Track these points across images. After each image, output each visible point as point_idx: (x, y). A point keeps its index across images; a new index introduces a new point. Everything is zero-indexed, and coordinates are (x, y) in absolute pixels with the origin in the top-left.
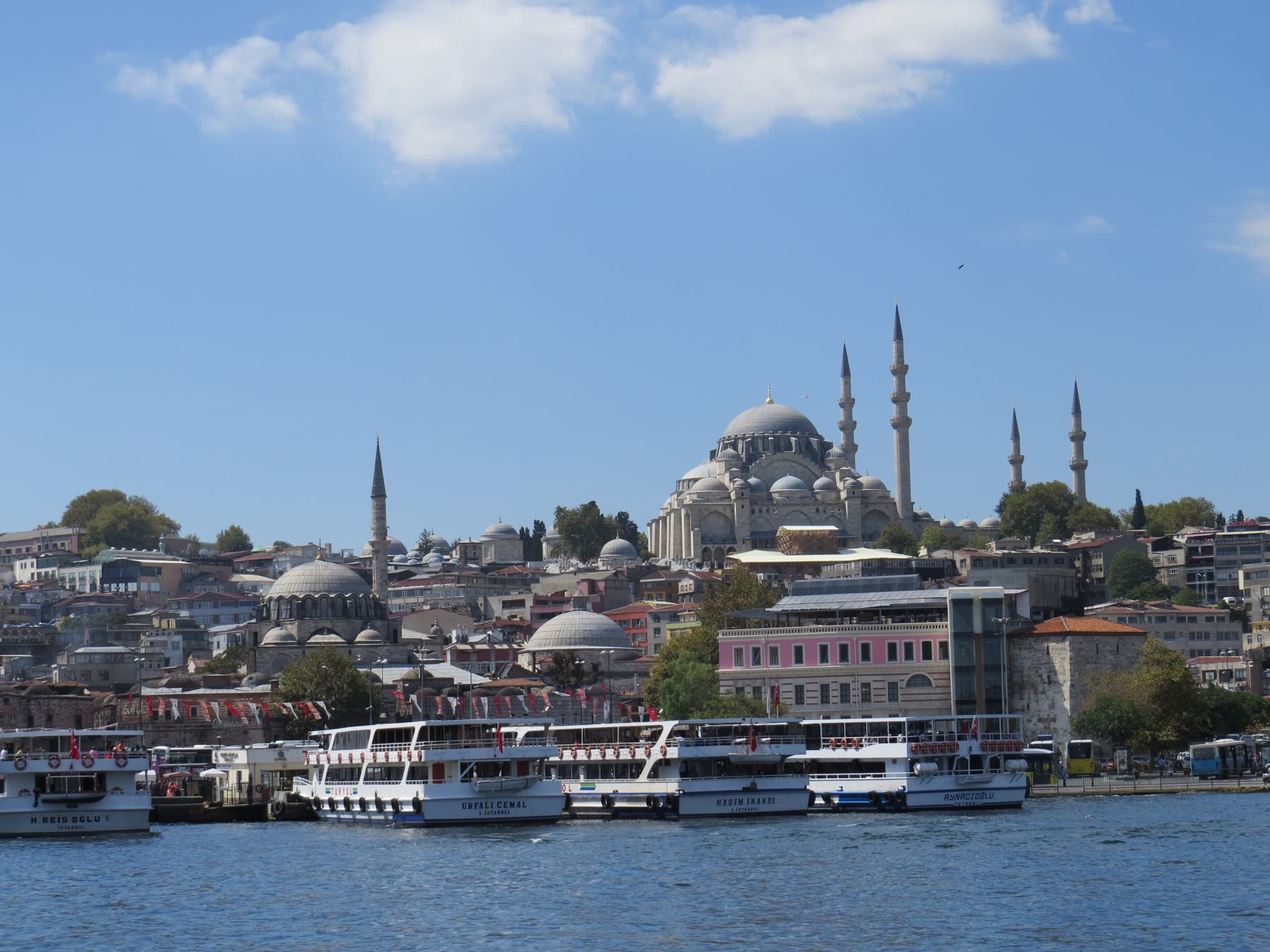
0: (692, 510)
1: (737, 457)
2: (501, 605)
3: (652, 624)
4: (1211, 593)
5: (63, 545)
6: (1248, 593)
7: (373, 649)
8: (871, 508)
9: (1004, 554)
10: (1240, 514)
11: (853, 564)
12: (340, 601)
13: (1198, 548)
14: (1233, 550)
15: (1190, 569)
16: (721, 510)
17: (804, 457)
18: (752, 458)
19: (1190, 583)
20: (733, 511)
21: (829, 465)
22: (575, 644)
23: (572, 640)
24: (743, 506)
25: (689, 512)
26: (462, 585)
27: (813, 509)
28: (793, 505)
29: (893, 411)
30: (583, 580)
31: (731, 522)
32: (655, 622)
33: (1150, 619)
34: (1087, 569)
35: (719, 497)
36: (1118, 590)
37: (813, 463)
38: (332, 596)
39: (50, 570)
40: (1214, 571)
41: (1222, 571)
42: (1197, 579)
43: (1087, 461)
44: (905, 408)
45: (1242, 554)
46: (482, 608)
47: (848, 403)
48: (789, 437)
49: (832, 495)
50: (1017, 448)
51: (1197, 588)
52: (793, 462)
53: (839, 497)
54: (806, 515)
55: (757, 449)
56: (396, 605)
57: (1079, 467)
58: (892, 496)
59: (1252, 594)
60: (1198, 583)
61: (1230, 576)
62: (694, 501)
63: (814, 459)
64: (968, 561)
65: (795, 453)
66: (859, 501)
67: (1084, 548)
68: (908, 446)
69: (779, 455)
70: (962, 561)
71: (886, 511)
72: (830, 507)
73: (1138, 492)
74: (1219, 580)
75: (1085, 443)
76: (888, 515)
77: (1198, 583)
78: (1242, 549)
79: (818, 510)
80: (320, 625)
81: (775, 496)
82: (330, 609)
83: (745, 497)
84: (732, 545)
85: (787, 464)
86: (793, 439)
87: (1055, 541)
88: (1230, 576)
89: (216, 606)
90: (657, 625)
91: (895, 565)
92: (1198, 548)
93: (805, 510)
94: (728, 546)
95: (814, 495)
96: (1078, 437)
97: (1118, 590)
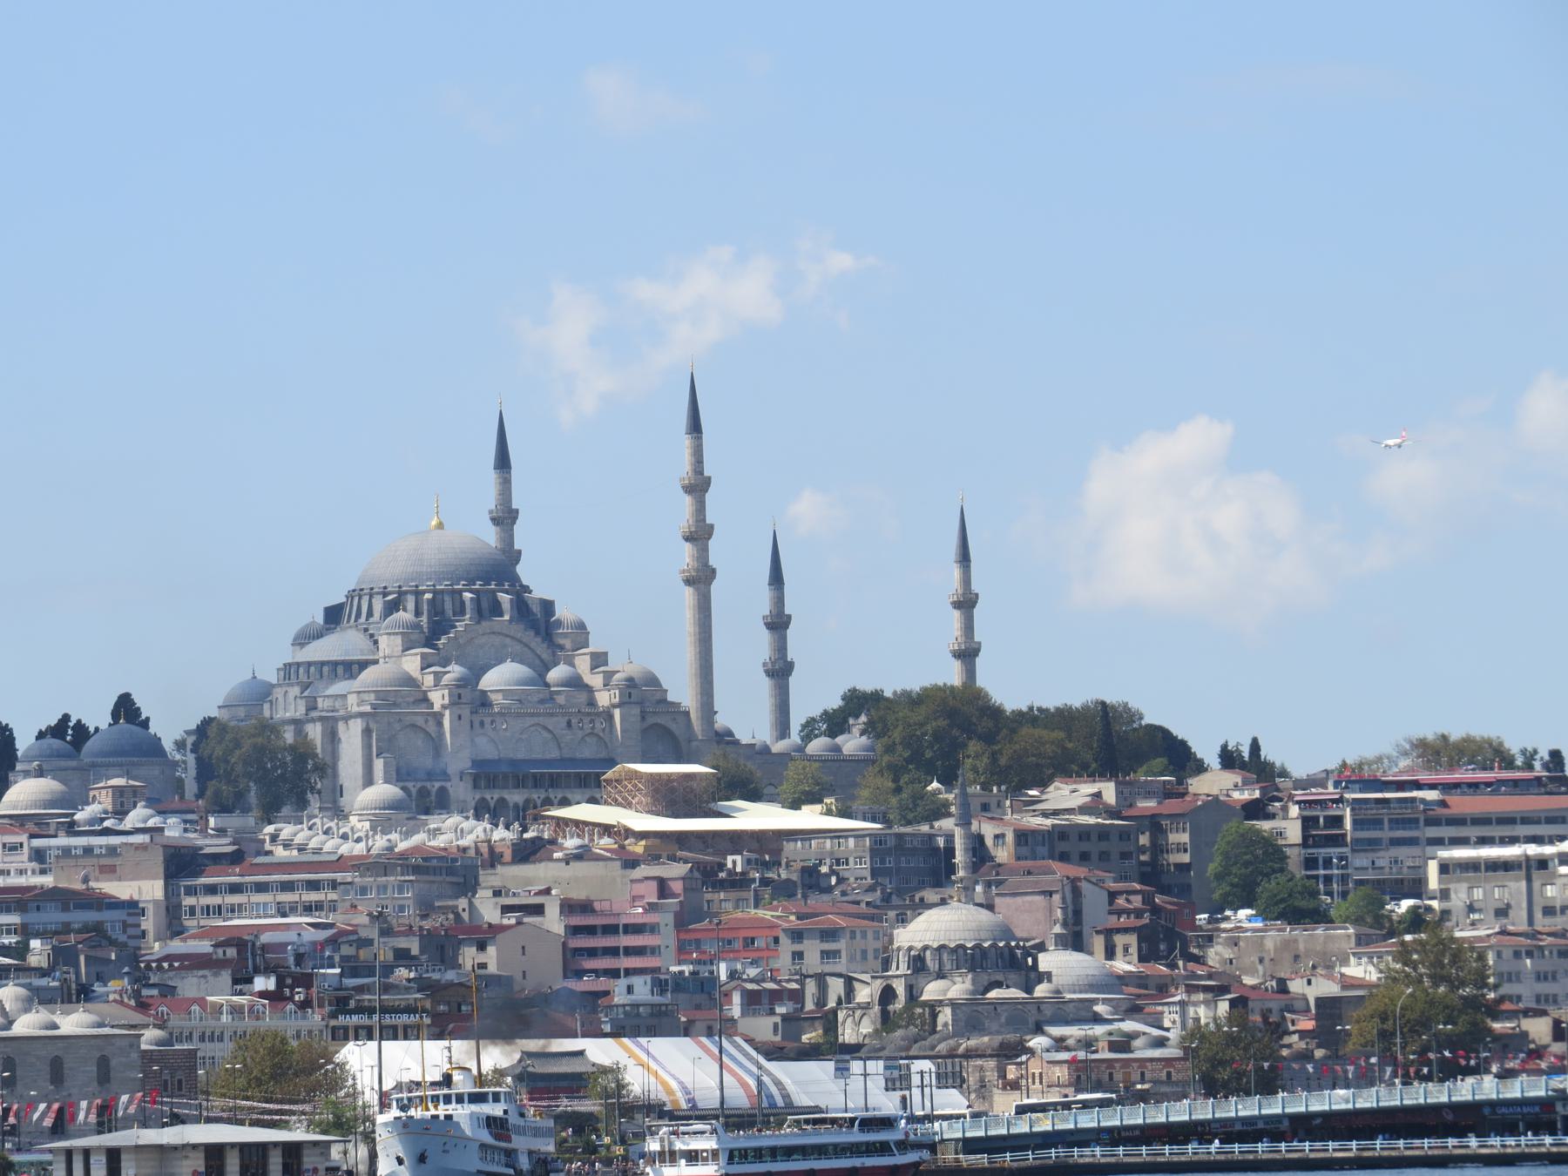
0: (377, 722)
1: (417, 626)
2: (499, 911)
3: (787, 946)
4: (1345, 888)
6: (1444, 895)
7: (1061, 1006)
8: (651, 720)
9: (1053, 826)
10: (1344, 762)
11: (851, 841)
12: (1007, 949)
13: (1317, 818)
14: (1376, 823)
15: (1310, 851)
16: (420, 721)
17: (525, 630)
18: (439, 627)
19: (1309, 873)
20: (440, 724)
21: (561, 641)
22: (1081, 992)
23: (1077, 988)
24: (460, 717)
25: (373, 726)
26: (407, 878)
27: (563, 721)
28: (532, 715)
30: (647, 878)
31: (436, 743)
32: (793, 943)
33: (1551, 953)
34: (1158, 848)
35: (412, 700)
36: (1232, 885)
37: (539, 640)
40: (1349, 855)
41: (1362, 854)
42: (1335, 867)
43: (980, 643)
45: (1391, 829)
46: (465, 916)
47: (505, 518)
48: (494, 592)
49: (582, 697)
50: (779, 601)
51: (1321, 880)
52: (507, 636)
53: (592, 703)
54: (550, 731)
55: (443, 612)
56: (258, 904)
57: (967, 654)
58: (670, 698)
59: (1453, 896)
60: (1322, 872)
61: (1373, 862)
62: (374, 707)
63: (537, 633)
64: (1010, 838)
65: (510, 621)
66: (636, 711)
67: (1153, 816)
68: (709, 616)
69: (485, 624)
70: (997, 837)
71: (673, 727)
72: (586, 720)
74: (1356, 869)
75: (976, 611)
76: (677, 732)
77: (1322, 872)
78: (1390, 821)
79: (569, 724)
81: (497, 699)
82: (999, 961)
83: (463, 700)
84: (443, 784)
85: (497, 640)
86: (467, 595)
87: (1031, 792)
88: (1373, 862)
89: (65, 909)
90: (798, 947)
91: (915, 843)
92: (1317, 818)
93: (550, 723)
94: (437, 785)
95: (551, 698)
96: (966, 603)
97: (1232, 885)
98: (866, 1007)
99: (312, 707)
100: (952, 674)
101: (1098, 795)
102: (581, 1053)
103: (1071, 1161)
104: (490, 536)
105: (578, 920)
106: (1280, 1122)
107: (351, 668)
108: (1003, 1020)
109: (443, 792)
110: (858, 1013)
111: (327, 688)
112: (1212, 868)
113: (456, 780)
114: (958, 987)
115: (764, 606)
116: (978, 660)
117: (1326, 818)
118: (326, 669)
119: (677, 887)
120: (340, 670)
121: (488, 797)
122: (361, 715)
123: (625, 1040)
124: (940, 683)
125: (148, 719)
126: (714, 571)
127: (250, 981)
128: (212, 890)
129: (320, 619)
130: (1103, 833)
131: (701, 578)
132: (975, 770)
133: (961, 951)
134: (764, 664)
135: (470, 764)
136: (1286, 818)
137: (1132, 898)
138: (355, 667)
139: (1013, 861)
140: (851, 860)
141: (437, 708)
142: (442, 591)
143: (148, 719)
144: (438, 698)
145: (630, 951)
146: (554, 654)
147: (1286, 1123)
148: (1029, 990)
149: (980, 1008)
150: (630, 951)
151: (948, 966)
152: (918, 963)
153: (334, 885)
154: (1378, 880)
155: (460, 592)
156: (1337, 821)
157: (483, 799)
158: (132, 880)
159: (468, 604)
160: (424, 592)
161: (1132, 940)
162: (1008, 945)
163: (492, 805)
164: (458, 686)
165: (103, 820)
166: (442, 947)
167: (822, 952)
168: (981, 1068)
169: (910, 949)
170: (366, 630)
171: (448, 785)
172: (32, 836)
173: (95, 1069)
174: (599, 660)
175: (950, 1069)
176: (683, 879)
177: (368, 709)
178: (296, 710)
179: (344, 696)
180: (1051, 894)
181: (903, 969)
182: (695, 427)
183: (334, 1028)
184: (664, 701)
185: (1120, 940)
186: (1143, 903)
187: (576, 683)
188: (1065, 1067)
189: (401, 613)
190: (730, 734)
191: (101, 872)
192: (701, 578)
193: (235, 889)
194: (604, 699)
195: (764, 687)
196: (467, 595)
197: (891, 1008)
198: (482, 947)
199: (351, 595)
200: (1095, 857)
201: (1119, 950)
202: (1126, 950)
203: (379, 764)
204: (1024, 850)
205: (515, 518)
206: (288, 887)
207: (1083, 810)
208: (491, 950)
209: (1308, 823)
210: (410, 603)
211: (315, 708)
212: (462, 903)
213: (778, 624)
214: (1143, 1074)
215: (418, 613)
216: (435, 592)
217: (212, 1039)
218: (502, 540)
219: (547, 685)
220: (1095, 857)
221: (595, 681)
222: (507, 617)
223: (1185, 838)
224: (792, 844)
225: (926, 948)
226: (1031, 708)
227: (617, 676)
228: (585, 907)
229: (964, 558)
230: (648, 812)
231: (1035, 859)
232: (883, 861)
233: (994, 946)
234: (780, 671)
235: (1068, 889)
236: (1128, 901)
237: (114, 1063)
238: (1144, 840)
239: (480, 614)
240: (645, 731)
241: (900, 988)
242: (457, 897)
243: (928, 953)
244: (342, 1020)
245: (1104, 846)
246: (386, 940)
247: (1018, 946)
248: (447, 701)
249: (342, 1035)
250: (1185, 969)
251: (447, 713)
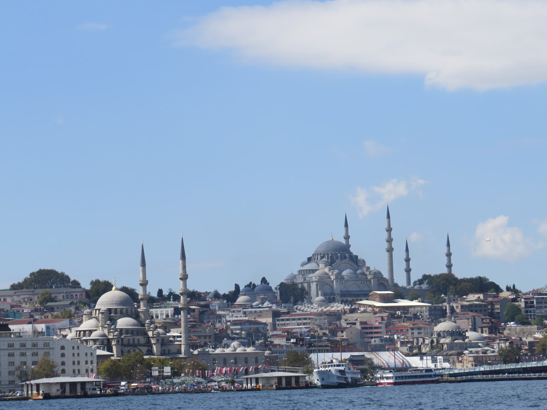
3: (410, 331)
5: (76, 295)
8: (380, 282)
9: (469, 304)
11: (424, 308)
14: (541, 303)
16: (329, 282)
20: (333, 283)
25: (318, 283)
27: (360, 282)
29: (386, 245)
31: (332, 287)
34: (493, 309)
36: (509, 317)
37: (355, 264)
38: (454, 330)
44: (391, 244)
45: (545, 304)
46: (339, 325)
47: (347, 237)
48: (344, 254)
49: (364, 277)
53: (366, 278)
56: (293, 323)
57: (449, 266)
58: (384, 277)
60: (529, 314)
62: (318, 279)
63: (354, 263)
64: (460, 307)
66: (376, 280)
67: (491, 302)
69: (343, 261)
70: (457, 307)
71: (384, 283)
76: (385, 284)
77: (529, 314)
78: (544, 302)
79: (362, 283)
80: (456, 338)
81: (345, 277)
89: (250, 324)
90: (412, 331)
92: (528, 302)
94: (333, 296)
95: (358, 277)
97: (509, 317)
98: (427, 345)
99: (305, 280)
100: (445, 271)
101: (479, 297)
102: (364, 355)
103: (473, 378)
104: (343, 241)
105: (363, 326)
106: (520, 369)
107: (313, 271)
108: (458, 347)
109: (334, 298)
110: (426, 346)
111: (308, 275)
112: (505, 313)
113: (337, 295)
114: (448, 340)
115: (404, 256)
116: (452, 268)
117: (530, 302)
118: (308, 271)
119: (386, 318)
120: (311, 271)
121: (344, 299)
122: (316, 281)
123: (374, 352)
124: (444, 273)
125: (269, 283)
126: (393, 249)
127: (290, 340)
128: (283, 320)
129: (306, 260)
130: (480, 306)
131: (390, 250)
132: (452, 292)
133: (448, 332)
134: (405, 269)
135: (339, 292)
136: (521, 302)
137: (487, 320)
138: (314, 271)
139: (460, 312)
140: (424, 312)
141: (332, 279)
142: (333, 254)
143: (269, 283)
144: (333, 277)
145: (375, 333)
146: (358, 267)
147: (522, 370)
148: (464, 340)
149: (453, 345)
150: (375, 333)
151: (446, 335)
152: (439, 335)
153: (310, 319)
154: (542, 316)
155: (337, 254)
156: (533, 302)
157: (343, 300)
158: (265, 318)
159: (339, 257)
160: (329, 254)
161: (487, 329)
162: (459, 330)
163: (345, 301)
164: (337, 275)
165: (259, 305)
166: (334, 332)
167: (418, 333)
168: (453, 358)
169: (437, 331)
170: (317, 263)
171: (335, 296)
172: (243, 309)
173: (254, 360)
174: (368, 268)
175: (446, 358)
176: (387, 316)
177: (317, 280)
178: (302, 281)
179: (312, 277)
180: (469, 319)
181: (436, 336)
182: (388, 217)
183: (309, 350)
184: (382, 277)
185: (484, 329)
186: (490, 321)
187: (363, 274)
188: (472, 358)
189: (324, 259)
190: (397, 284)
191: (258, 316)
192: (390, 250)
193: (288, 320)
194: (369, 277)
195: (405, 274)
196: (339, 255)
197: (433, 345)
198: (342, 332)
199: (313, 255)
200: (479, 311)
201: (484, 331)
202: (486, 331)
203: (320, 292)
204: (463, 309)
205: (349, 238)
206: (299, 319)
207: (476, 300)
208: (344, 333)
209: (526, 303)
210: (326, 257)
211: (305, 280)
212: (338, 322)
213: (408, 260)
214: (490, 359)
215: (328, 259)
216: (332, 254)
217: (281, 353)
218: (346, 242)
219: (357, 274)
220: (479, 311)
221: (368, 273)
222: (348, 259)
223: (498, 306)
224: (411, 309)
225: (441, 331)
226: (464, 278)
227: (372, 272)
228: (365, 323)
229: (448, 245)
230: (379, 302)
231: (465, 311)
232: (431, 312)
233: (456, 331)
234: (408, 270)
235: (473, 318)
236: (486, 321)
237: (259, 359)
238: (489, 307)
239: (342, 259)
240: (378, 284)
241: (435, 340)
242: (337, 321)
243: (441, 332)
244: (311, 348)
245: (481, 308)
246: (321, 331)
247: (461, 331)
248: (334, 278)
249: (311, 352)
250: (499, 335)
251: (335, 281)
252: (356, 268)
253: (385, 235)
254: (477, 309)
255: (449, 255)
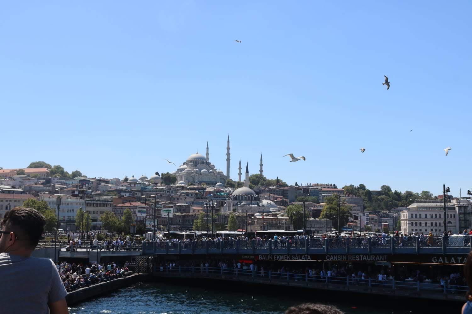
8: (221, 177)
39: (63, 181)
57: (261, 171)
58: (225, 175)
73: (278, 177)
96: (261, 165)
100: (259, 173)
104: (205, 156)
131: (228, 160)
192: (228, 160)
195: (238, 176)
252: (209, 169)
253: (226, 152)
254: (274, 192)
255: (261, 165)
